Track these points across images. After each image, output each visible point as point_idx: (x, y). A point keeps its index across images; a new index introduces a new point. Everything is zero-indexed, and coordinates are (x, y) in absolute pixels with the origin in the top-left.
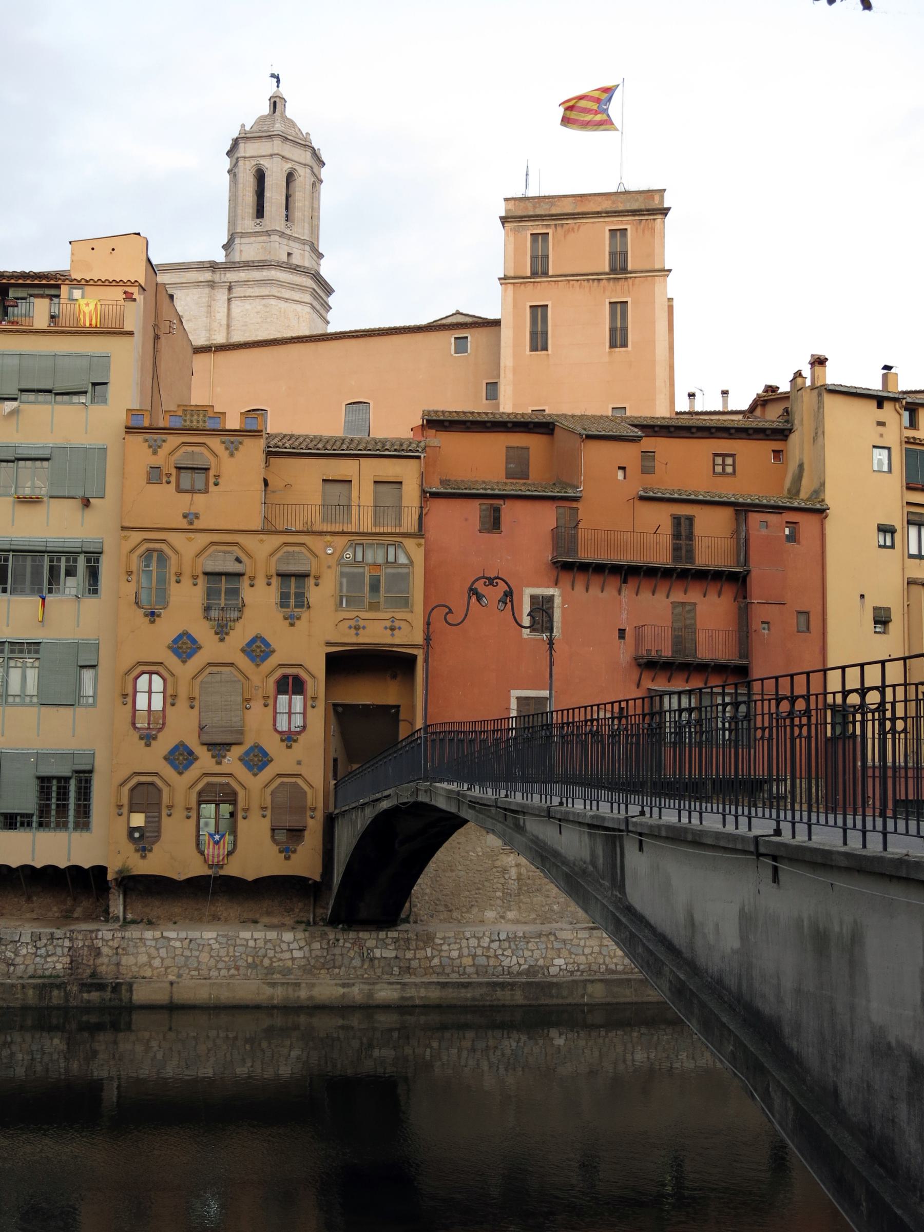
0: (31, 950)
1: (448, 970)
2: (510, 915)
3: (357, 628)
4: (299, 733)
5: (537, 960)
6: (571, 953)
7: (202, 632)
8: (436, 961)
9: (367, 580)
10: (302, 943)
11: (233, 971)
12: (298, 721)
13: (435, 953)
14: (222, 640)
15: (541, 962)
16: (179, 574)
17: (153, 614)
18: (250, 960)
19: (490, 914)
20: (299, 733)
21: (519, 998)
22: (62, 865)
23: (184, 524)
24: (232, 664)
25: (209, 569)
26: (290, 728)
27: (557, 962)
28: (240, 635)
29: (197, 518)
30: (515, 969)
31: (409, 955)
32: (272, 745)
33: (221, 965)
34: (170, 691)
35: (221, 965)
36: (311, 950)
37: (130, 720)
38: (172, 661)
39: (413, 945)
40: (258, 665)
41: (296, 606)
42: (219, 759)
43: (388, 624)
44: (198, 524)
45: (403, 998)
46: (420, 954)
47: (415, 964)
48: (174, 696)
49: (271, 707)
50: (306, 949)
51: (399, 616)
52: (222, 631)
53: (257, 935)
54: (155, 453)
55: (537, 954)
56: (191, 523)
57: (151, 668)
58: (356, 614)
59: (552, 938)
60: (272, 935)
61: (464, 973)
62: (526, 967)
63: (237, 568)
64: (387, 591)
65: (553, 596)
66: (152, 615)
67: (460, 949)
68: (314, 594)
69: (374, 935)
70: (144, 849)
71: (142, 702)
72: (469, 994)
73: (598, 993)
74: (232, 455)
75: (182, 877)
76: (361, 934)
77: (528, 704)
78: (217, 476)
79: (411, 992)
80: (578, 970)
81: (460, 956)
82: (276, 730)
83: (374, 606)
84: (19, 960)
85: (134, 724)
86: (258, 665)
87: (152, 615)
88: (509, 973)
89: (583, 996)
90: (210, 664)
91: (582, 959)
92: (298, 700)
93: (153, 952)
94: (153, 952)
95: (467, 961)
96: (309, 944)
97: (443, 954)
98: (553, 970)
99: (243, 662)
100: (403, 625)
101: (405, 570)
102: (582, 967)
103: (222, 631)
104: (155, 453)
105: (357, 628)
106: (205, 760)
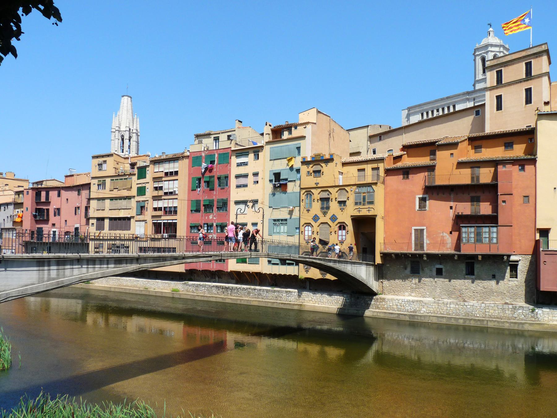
0: (286, 295)
1: (389, 309)
2: (413, 294)
3: (359, 211)
4: (344, 241)
5: (416, 308)
6: (428, 307)
7: (320, 214)
8: (386, 306)
9: (362, 197)
10: (349, 298)
11: (331, 304)
12: (344, 237)
13: (385, 303)
14: (325, 216)
15: (418, 309)
16: (314, 199)
17: (308, 210)
18: (336, 301)
19: (407, 294)
20: (344, 241)
21: (407, 318)
23: (315, 186)
24: (327, 223)
25: (321, 197)
26: (342, 239)
27: (423, 309)
28: (329, 214)
29: (318, 184)
30: (409, 310)
31: (378, 303)
33: (329, 302)
34: (312, 230)
35: (329, 302)
36: (351, 300)
37: (303, 238)
38: (313, 223)
39: (379, 301)
40: (333, 223)
41: (344, 206)
43: (368, 209)
44: (319, 186)
45: (373, 315)
46: (381, 303)
47: (380, 306)
48: (313, 232)
49: (337, 234)
50: (350, 299)
51: (370, 207)
52: (325, 214)
54: (308, 168)
55: (416, 307)
56: (317, 185)
57: (308, 224)
58: (359, 207)
59: (422, 302)
61: (394, 310)
62: (413, 310)
63: (328, 197)
64: (368, 200)
65: (426, 197)
66: (308, 211)
67: (393, 303)
68: (347, 203)
69: (368, 297)
70: (307, 271)
71: (306, 233)
72: (392, 316)
73: (435, 320)
74: (326, 166)
75: (316, 279)
76: (365, 297)
77: (418, 231)
78: (323, 172)
79: (375, 314)
80: (430, 313)
81: (393, 305)
82: (338, 240)
83: (364, 205)
84: (283, 297)
85: (304, 239)
86: (333, 223)
87: (308, 211)
88: (408, 311)
89: (429, 321)
90: (322, 223)
91: (432, 309)
92: (344, 232)
93: (312, 297)
94: (312, 297)
95: (395, 307)
96: (351, 298)
97: (388, 304)
98: (421, 312)
99: (330, 222)
100: (372, 209)
101: (372, 193)
102: (431, 312)
103: (325, 214)
104: (308, 168)
105: (359, 211)
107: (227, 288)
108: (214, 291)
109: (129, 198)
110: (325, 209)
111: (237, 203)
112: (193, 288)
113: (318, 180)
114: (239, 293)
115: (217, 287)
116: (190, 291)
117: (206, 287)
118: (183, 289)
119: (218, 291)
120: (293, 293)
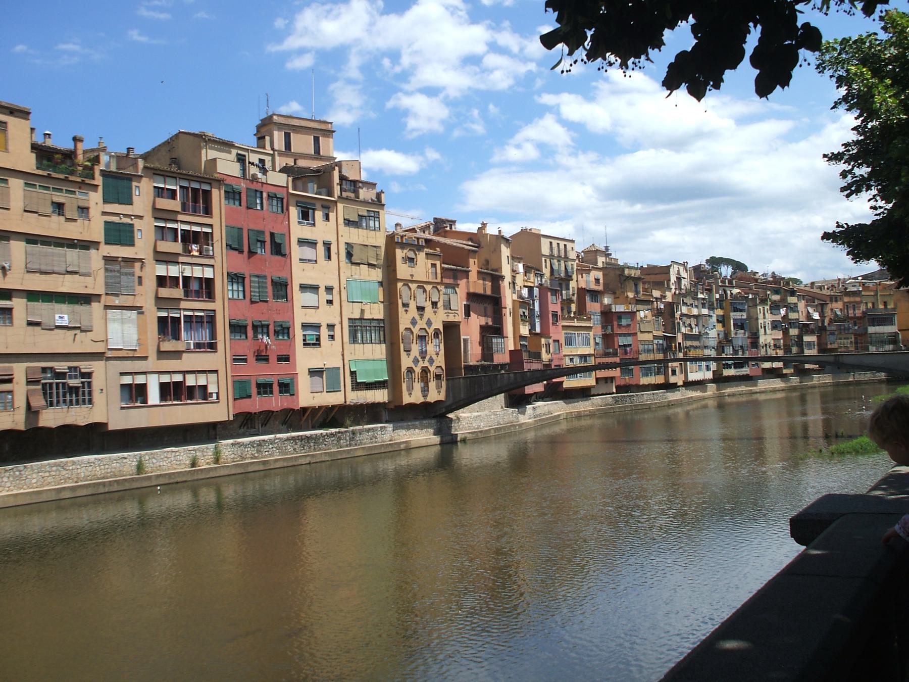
3: (448, 316)
7: (417, 318)
22: (382, 402)
32: (434, 357)
42: (423, 360)
44: (414, 279)
52: (421, 316)
53: (427, 422)
60: (430, 421)
84: (378, 436)
103: (421, 316)
105: (448, 316)
106: (421, 362)
107: (308, 438)
108: (289, 447)
109: (86, 245)
110: (421, 309)
111: (304, 288)
112: (253, 449)
113: (413, 271)
114: (326, 443)
115: (293, 438)
116: (248, 456)
117: (275, 443)
118: (233, 456)
119: (296, 447)
120: (388, 429)
